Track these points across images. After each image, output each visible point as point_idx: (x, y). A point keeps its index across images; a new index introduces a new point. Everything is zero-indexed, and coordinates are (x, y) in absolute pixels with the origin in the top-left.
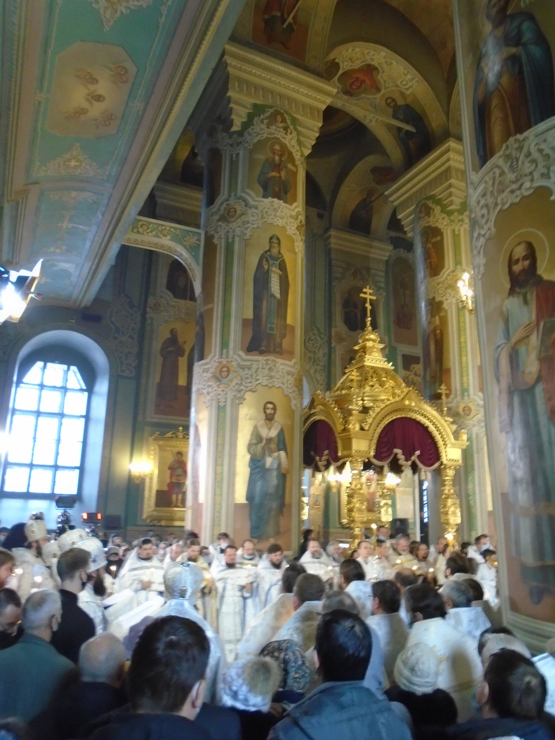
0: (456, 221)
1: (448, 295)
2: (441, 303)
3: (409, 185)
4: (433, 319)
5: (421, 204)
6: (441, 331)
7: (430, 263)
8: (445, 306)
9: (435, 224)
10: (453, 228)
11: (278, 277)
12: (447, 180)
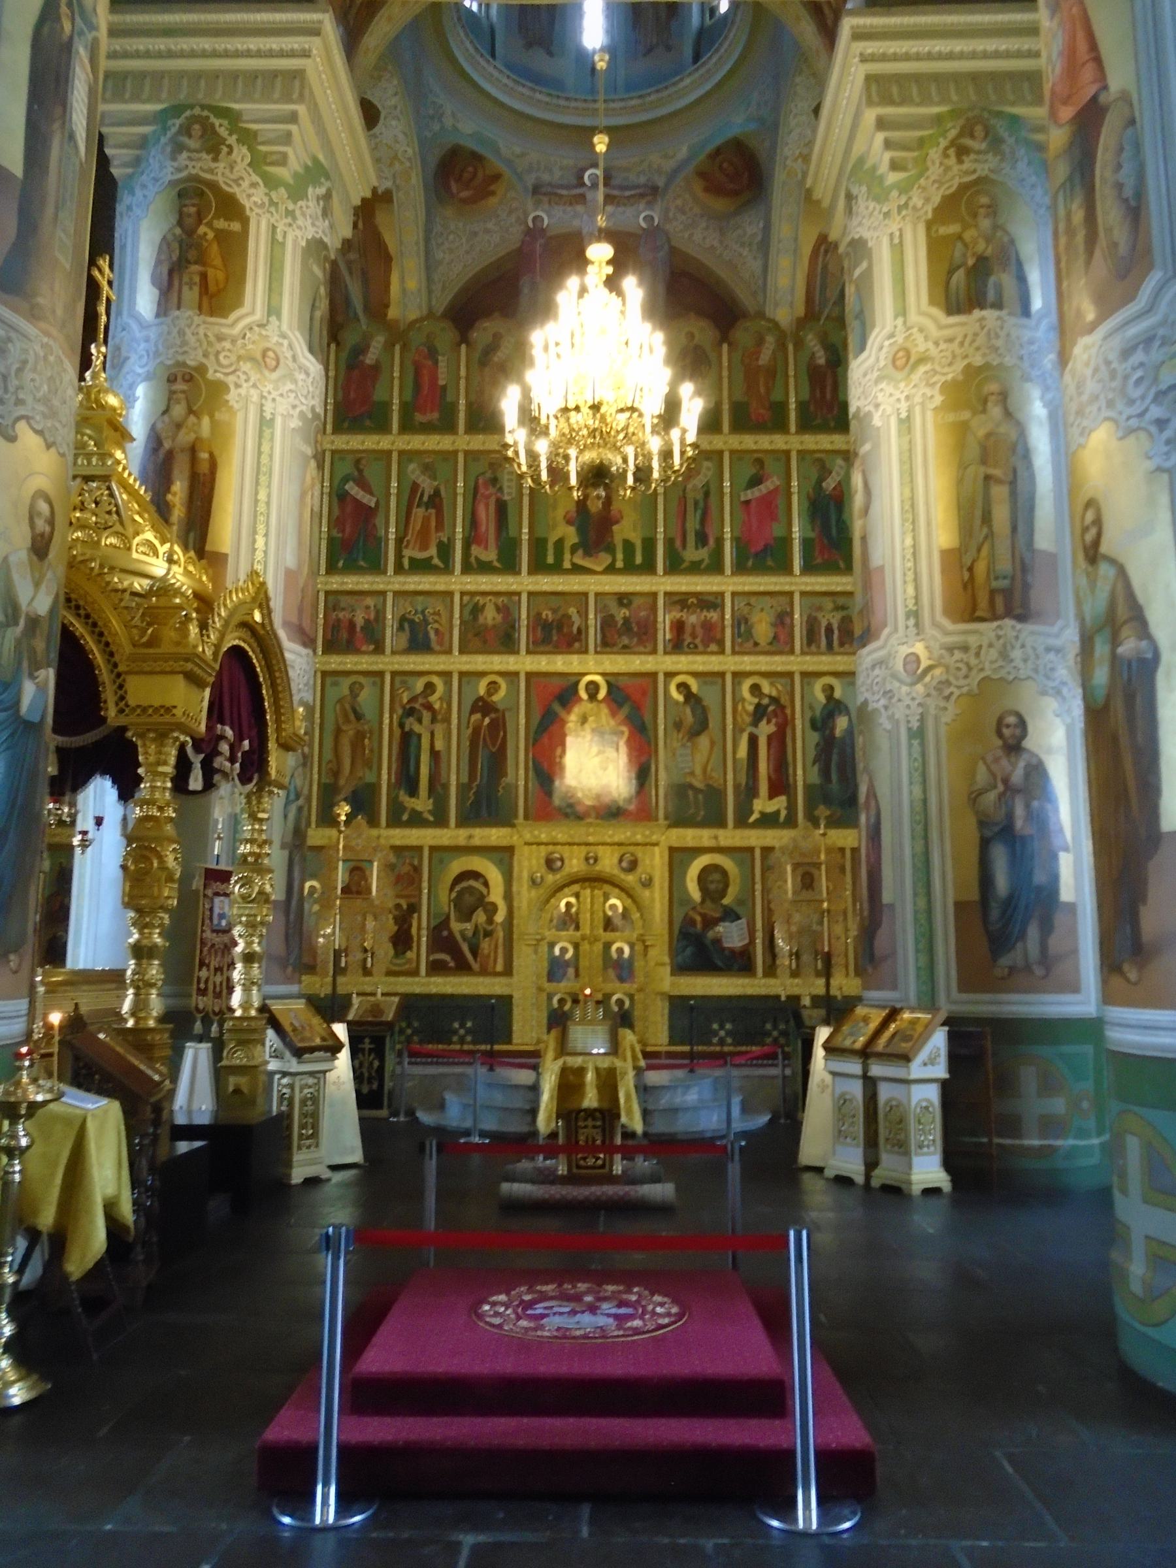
0: (282, 208)
1: (243, 377)
2: (219, 388)
3: (161, 44)
4: (192, 419)
5: (188, 113)
6: (211, 455)
7: (204, 276)
8: (232, 396)
9: (230, 186)
10: (272, 220)
11: (87, 89)
12: (287, 98)
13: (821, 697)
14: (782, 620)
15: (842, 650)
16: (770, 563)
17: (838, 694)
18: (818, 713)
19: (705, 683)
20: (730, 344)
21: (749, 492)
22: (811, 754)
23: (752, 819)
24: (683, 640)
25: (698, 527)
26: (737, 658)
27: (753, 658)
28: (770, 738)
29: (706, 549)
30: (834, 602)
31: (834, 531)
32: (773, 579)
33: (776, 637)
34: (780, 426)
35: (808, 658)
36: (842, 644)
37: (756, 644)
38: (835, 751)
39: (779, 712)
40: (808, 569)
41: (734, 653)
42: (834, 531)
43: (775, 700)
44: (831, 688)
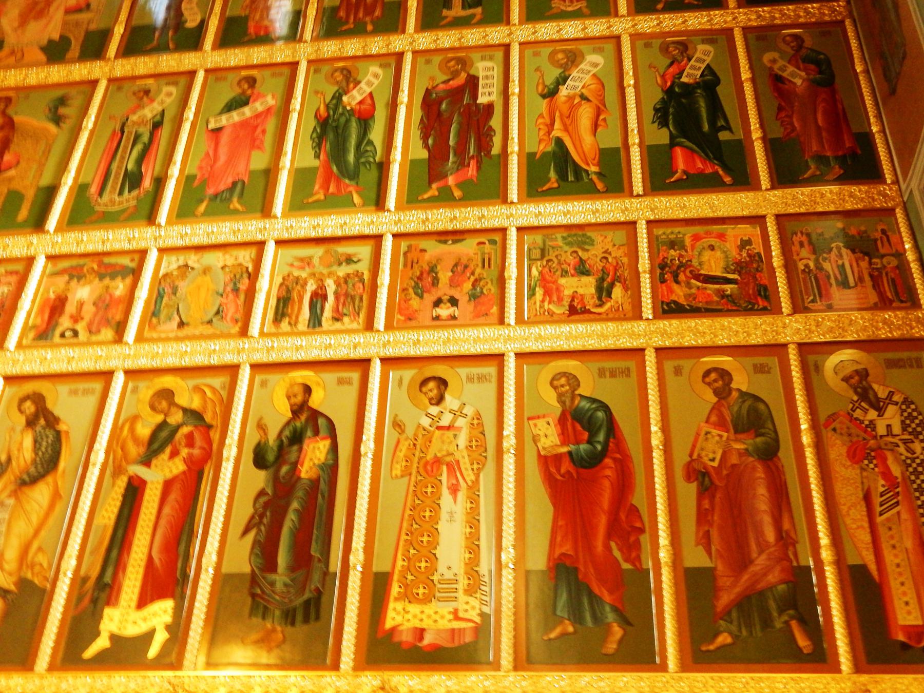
15: (338, 325)
16: (235, 204)
19: (74, 392)
22: (245, 510)
24: (57, 324)
25: (130, 167)
28: (168, 485)
29: (135, 193)
31: (351, 157)
36: (337, 318)
38: (295, 505)
39: (198, 437)
42: (351, 157)
43: (194, 415)
44: (308, 390)
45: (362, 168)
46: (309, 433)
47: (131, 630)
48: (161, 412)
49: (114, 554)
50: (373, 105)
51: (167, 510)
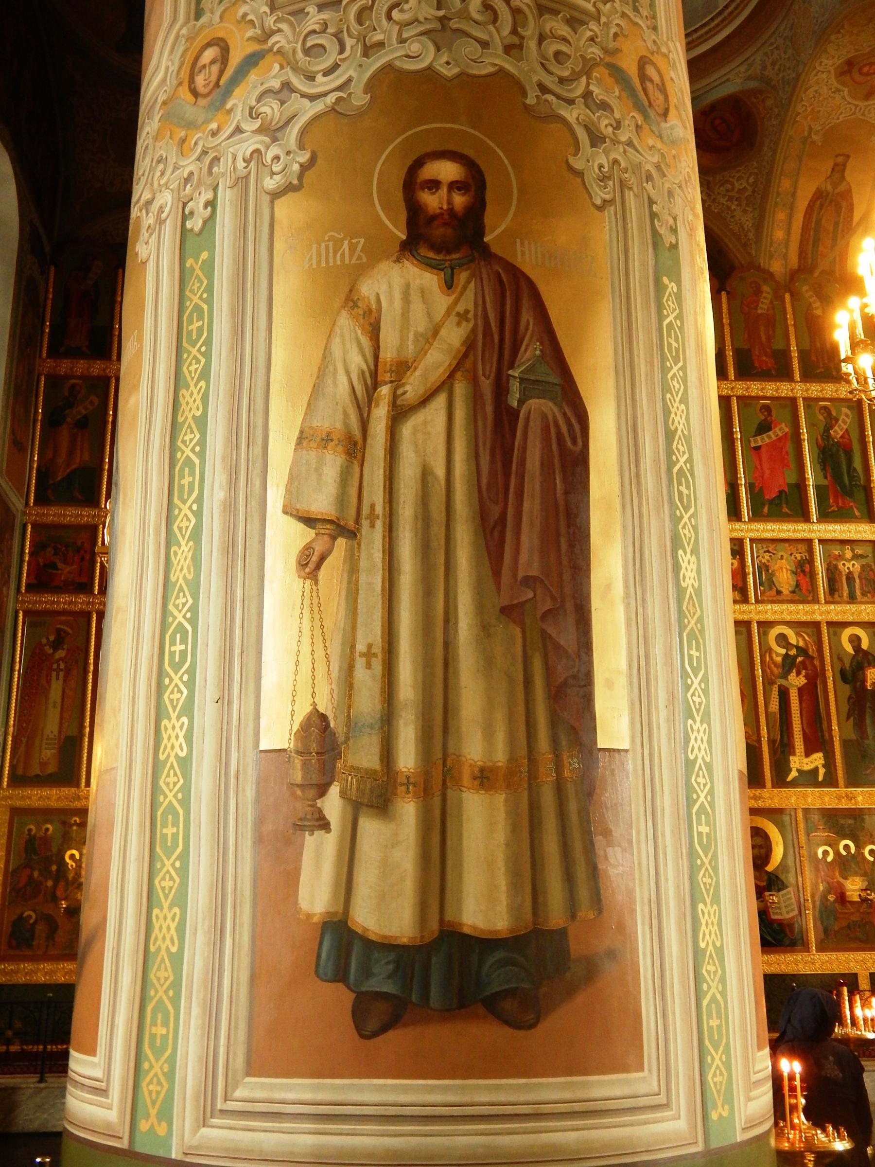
13: (849, 649)
14: (805, 568)
15: (865, 599)
16: (786, 510)
17: (865, 645)
18: (847, 665)
20: (728, 293)
21: (758, 438)
22: (845, 708)
23: (789, 779)
26: (761, 607)
27: (776, 607)
28: (800, 690)
30: (852, 550)
32: (790, 526)
33: (797, 586)
34: (785, 375)
35: (832, 607)
37: (779, 592)
38: (868, 704)
40: (825, 516)
41: (757, 601)
43: (802, 651)
44: (859, 639)
45: (855, 489)
46: (866, 664)
47: (806, 768)
48: (783, 648)
49: (785, 728)
50: (850, 440)
51: (804, 705)
